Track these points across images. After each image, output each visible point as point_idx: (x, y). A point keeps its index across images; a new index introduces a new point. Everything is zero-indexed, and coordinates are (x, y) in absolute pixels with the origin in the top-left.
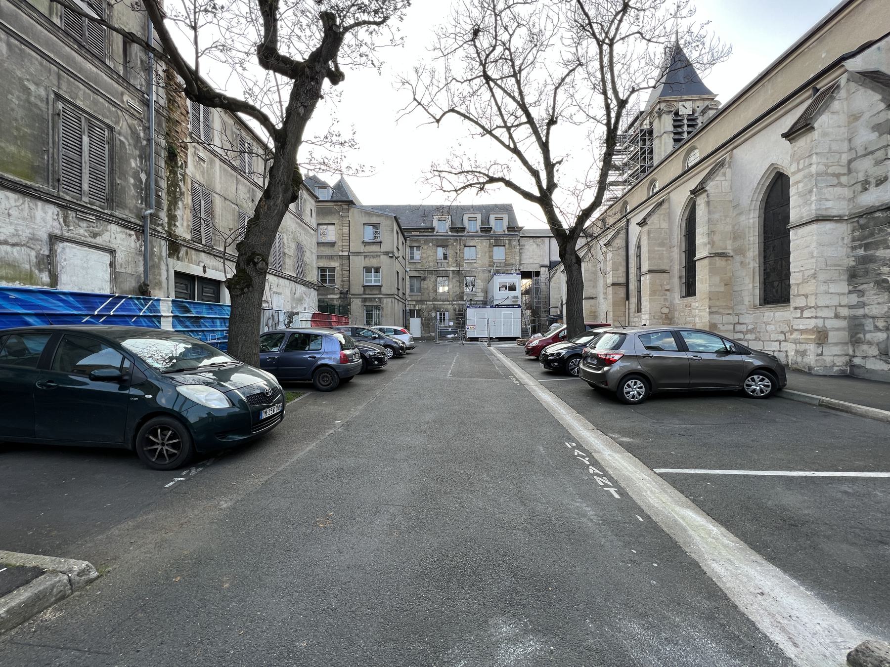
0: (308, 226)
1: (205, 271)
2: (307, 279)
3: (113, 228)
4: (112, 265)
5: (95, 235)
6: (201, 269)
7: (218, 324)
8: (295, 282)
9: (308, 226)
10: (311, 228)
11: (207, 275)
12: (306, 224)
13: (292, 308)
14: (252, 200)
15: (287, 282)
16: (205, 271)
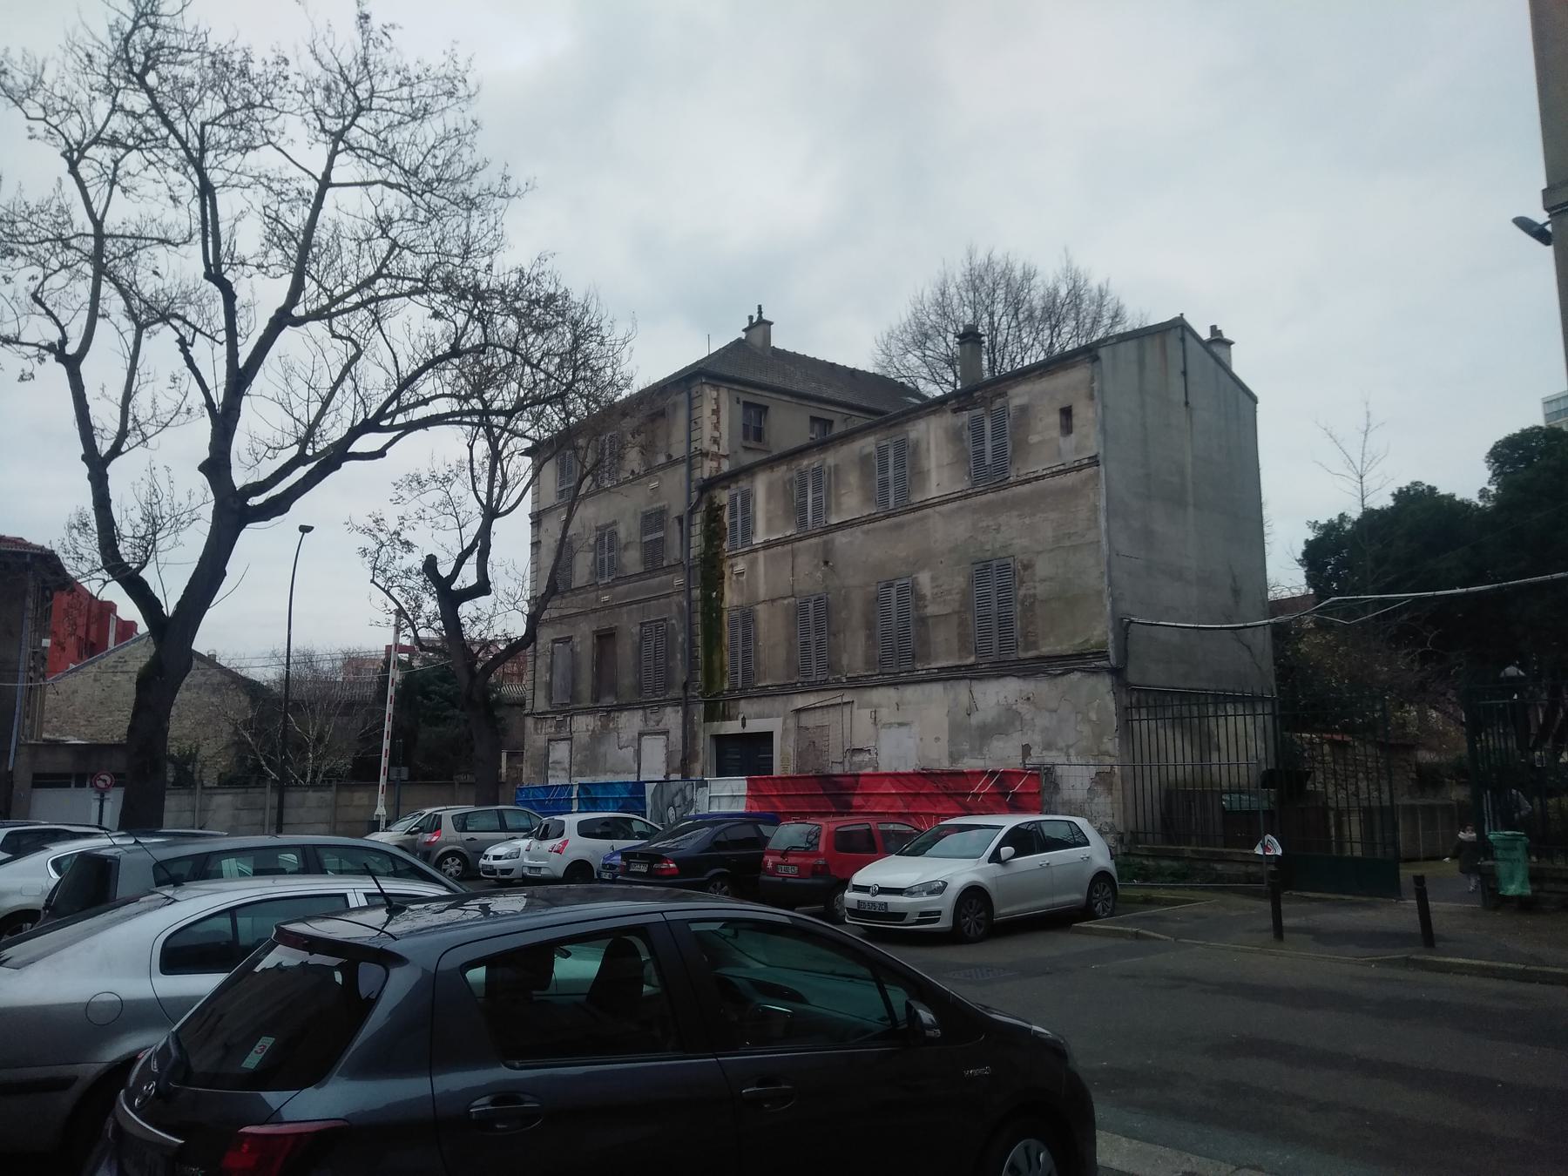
0: (1037, 479)
1: (744, 725)
2: (1045, 650)
3: (669, 710)
4: (667, 746)
5: (658, 723)
6: (740, 722)
7: (611, 805)
8: (971, 679)
9: (1037, 479)
10: (1053, 474)
11: (747, 730)
12: (1028, 481)
13: (953, 757)
14: (826, 563)
15: (936, 689)
16: (744, 725)
